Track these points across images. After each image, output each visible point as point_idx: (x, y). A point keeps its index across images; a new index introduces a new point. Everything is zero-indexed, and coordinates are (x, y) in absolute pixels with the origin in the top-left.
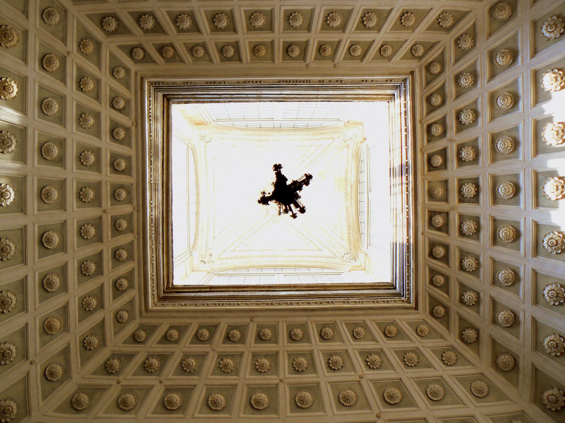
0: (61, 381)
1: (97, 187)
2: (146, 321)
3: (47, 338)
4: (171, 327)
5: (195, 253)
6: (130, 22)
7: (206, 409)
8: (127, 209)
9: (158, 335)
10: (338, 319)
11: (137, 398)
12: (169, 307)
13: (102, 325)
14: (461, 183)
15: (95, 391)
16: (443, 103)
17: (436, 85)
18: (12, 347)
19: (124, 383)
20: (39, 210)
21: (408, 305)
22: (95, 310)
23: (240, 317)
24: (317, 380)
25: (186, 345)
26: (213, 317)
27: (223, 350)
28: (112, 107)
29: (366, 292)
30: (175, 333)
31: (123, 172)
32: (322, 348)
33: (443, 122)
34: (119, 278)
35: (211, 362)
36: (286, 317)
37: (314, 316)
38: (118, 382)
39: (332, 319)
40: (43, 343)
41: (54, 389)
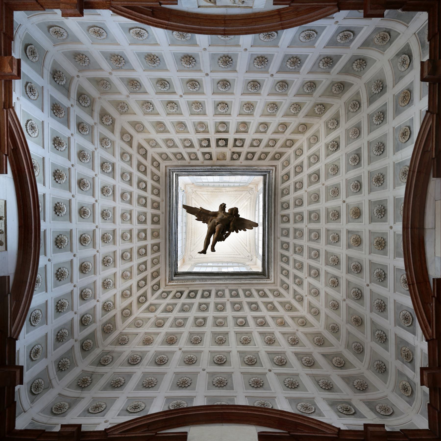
5: (247, 263)
6: (142, 291)
7: (318, 259)
21: (274, 170)
24: (306, 211)
26: (277, 255)
27: (292, 251)
29: (267, 188)
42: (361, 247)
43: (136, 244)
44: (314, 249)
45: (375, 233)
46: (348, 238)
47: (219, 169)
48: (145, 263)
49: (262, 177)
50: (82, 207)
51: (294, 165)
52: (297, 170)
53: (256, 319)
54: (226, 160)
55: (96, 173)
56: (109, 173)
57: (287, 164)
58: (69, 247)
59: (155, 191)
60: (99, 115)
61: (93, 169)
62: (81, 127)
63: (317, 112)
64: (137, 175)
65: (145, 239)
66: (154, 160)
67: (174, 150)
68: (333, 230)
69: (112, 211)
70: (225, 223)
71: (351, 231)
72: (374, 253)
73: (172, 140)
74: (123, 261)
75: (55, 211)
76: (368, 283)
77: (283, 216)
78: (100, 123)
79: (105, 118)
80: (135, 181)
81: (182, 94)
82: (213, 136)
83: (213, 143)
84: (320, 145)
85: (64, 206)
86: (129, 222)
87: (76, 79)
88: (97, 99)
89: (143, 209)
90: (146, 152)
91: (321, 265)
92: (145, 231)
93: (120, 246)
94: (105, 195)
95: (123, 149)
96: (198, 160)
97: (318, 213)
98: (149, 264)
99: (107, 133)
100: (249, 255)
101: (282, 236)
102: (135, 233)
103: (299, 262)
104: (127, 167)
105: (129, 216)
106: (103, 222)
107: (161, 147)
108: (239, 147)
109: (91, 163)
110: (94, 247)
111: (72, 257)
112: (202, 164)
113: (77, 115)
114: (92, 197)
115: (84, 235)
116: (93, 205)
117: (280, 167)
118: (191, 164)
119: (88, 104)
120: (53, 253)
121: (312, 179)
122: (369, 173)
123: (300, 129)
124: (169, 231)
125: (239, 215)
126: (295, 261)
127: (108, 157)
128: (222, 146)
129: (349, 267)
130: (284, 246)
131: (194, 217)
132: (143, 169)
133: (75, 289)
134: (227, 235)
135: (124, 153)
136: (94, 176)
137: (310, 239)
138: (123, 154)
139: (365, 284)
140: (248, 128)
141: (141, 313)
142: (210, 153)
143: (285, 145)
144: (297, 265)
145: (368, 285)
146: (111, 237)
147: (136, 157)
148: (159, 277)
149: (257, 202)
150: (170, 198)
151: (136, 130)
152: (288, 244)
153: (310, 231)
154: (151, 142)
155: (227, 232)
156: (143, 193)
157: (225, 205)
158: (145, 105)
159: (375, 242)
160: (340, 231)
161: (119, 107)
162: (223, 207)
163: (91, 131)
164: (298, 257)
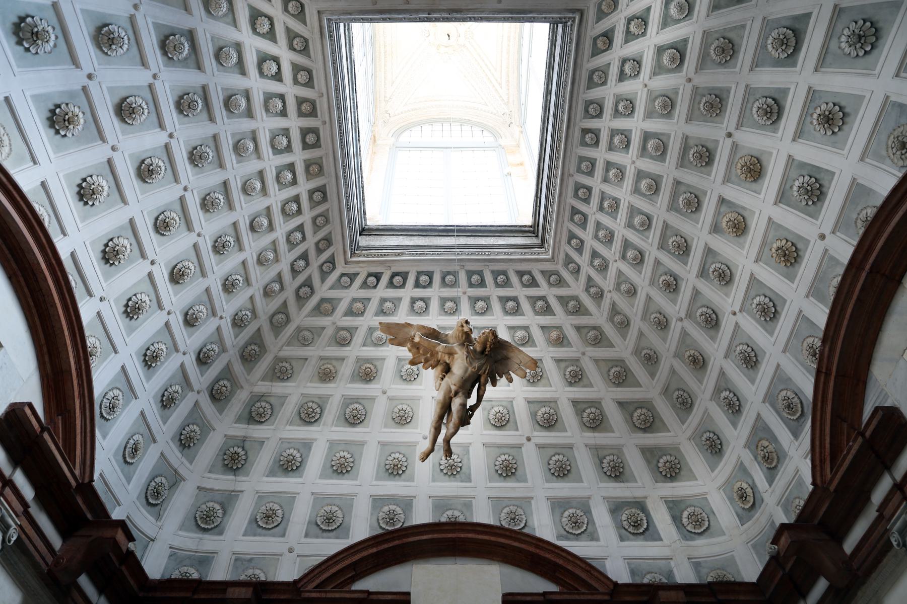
2: (561, 261)
3: (565, 341)
4: (569, 243)
7: (646, 233)
9: (574, 255)
12: (550, 241)
13: (560, 298)
15: (614, 310)
18: (569, 370)
19: (611, 288)
22: (547, 302)
23: (567, 186)
26: (564, 208)
27: (595, 207)
28: (375, 287)
30: (574, 242)
31: (431, 278)
32: (608, 118)
34: (522, 282)
35: (606, 220)
36: (572, 146)
37: (575, 119)
39: (580, 102)
40: (569, 344)
41: (607, 338)
42: (741, 240)
43: (277, 196)
45: (780, 226)
46: (717, 213)
48: (300, 228)
53: (512, 331)
69: (212, 144)
71: (729, 202)
72: (766, 264)
74: (255, 234)
75: (81, 199)
77: (585, 131)
85: (100, 179)
89: (280, 123)
91: (650, 244)
97: (664, 140)
101: (578, 172)
103: (607, 228)
106: (197, 174)
110: (189, 228)
115: (162, 217)
120: (106, 281)
122: (809, 92)
124: (343, 162)
126: (598, 225)
129: (707, 267)
130: (580, 192)
133: (172, 318)
137: (636, 191)
139: (730, 309)
141: (306, 316)
144: (601, 234)
145: (734, 314)
146: (221, 197)
148: (331, 248)
150: (337, 89)
152: (589, 189)
156: (274, 87)
160: (705, 193)
164: (606, 220)
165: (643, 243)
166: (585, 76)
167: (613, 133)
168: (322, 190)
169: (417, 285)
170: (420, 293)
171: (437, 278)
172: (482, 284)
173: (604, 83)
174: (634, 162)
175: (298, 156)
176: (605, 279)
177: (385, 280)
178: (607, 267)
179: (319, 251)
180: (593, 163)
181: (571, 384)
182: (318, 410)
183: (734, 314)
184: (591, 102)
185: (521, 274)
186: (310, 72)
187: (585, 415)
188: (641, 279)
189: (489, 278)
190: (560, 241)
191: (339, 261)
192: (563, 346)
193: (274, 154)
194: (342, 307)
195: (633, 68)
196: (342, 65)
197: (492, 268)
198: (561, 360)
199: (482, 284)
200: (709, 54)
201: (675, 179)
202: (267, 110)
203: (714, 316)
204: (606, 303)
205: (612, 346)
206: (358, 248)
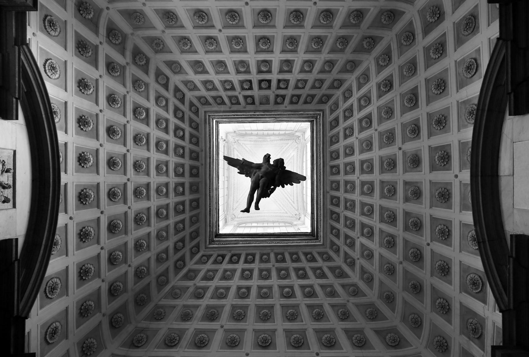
0: (358, 288)
1: (261, 271)
2: (328, 246)
4: (332, 233)
8: (272, 256)
10: (328, 150)
11: (366, 250)
12: (321, 234)
14: (260, 88)
15: (363, 271)
16: (221, 97)
17: (211, 100)
18: (340, 311)
19: (359, 257)
20: (272, 298)
22: (323, 271)
23: (327, 199)
25: (340, 225)
28: (221, 263)
29: (315, 136)
30: (334, 231)
31: (254, 257)
33: (230, 98)
34: (307, 259)
35: (349, 214)
38: (358, 259)
39: (328, 153)
40: (338, 296)
41: (362, 291)
43: (172, 200)
44: (366, 204)
46: (405, 191)
47: (263, 115)
48: (183, 221)
49: (309, 123)
50: (112, 158)
51: (342, 109)
52: (347, 114)
54: (269, 104)
55: (128, 119)
56: (143, 119)
57: (335, 107)
58: (95, 203)
59: (194, 140)
60: (131, 54)
61: (125, 115)
62: (111, 67)
63: (366, 47)
64: (173, 121)
65: (183, 193)
66: (192, 104)
67: (214, 93)
68: (388, 182)
69: (146, 162)
70: (270, 177)
72: (436, 207)
73: (211, 82)
76: (429, 242)
78: (133, 63)
79: (138, 57)
80: (171, 128)
81: (221, 28)
82: (255, 77)
83: (255, 86)
84: (371, 85)
86: (165, 174)
87: (105, 12)
88: (130, 36)
90: (184, 95)
91: (375, 222)
92: (182, 185)
93: (155, 202)
94: (138, 144)
95: (158, 93)
96: (240, 104)
98: (187, 222)
99: (140, 74)
100: (297, 213)
102: (172, 187)
103: (351, 219)
104: (163, 113)
105: (165, 168)
107: (200, 90)
108: (283, 89)
109: (122, 108)
110: (125, 202)
111: (99, 215)
112: (244, 109)
113: (106, 54)
114: (123, 146)
116: (125, 156)
117: (328, 112)
118: (232, 109)
119: (120, 41)
121: (364, 124)
123: (348, 67)
125: (285, 167)
126: (346, 218)
127: (142, 101)
128: (265, 89)
131: (236, 170)
132: (181, 115)
134: (273, 190)
135: (159, 97)
136: (126, 123)
137: (363, 193)
138: (158, 98)
139: (425, 243)
140: (292, 67)
142: (252, 97)
143: (332, 87)
144: (348, 223)
146: (145, 191)
147: (173, 101)
149: (305, 153)
151: (172, 71)
153: (363, 184)
154: (189, 85)
155: (272, 187)
157: (270, 155)
158: (182, 42)
159: (437, 194)
160: (396, 183)
161: (154, 45)
162: (267, 158)
163: (122, 73)
164: (349, 214)
165: (371, 222)
166: (328, 139)
167: (346, 165)
168: (197, 200)
169: (246, 262)
170: (247, 266)
171: (257, 257)
172: (283, 260)
173: (338, 142)
174: (358, 178)
175: (187, 180)
176: (355, 251)
177: (227, 259)
178: (354, 243)
179: (192, 239)
180: (338, 183)
181: (342, 320)
182: (178, 338)
183: (428, 244)
184: (333, 152)
185: (306, 254)
186: (198, 139)
187: (354, 338)
188: (374, 245)
189: (287, 257)
190: (326, 233)
191: (202, 246)
192: (335, 297)
193: (175, 176)
194: (201, 274)
195: (350, 132)
196: (213, 138)
197: (289, 251)
198: (335, 306)
199: (283, 260)
200: (382, 117)
201: (380, 180)
202: (175, 153)
203: (418, 252)
204: (357, 267)
205: (365, 295)
206: (214, 241)
